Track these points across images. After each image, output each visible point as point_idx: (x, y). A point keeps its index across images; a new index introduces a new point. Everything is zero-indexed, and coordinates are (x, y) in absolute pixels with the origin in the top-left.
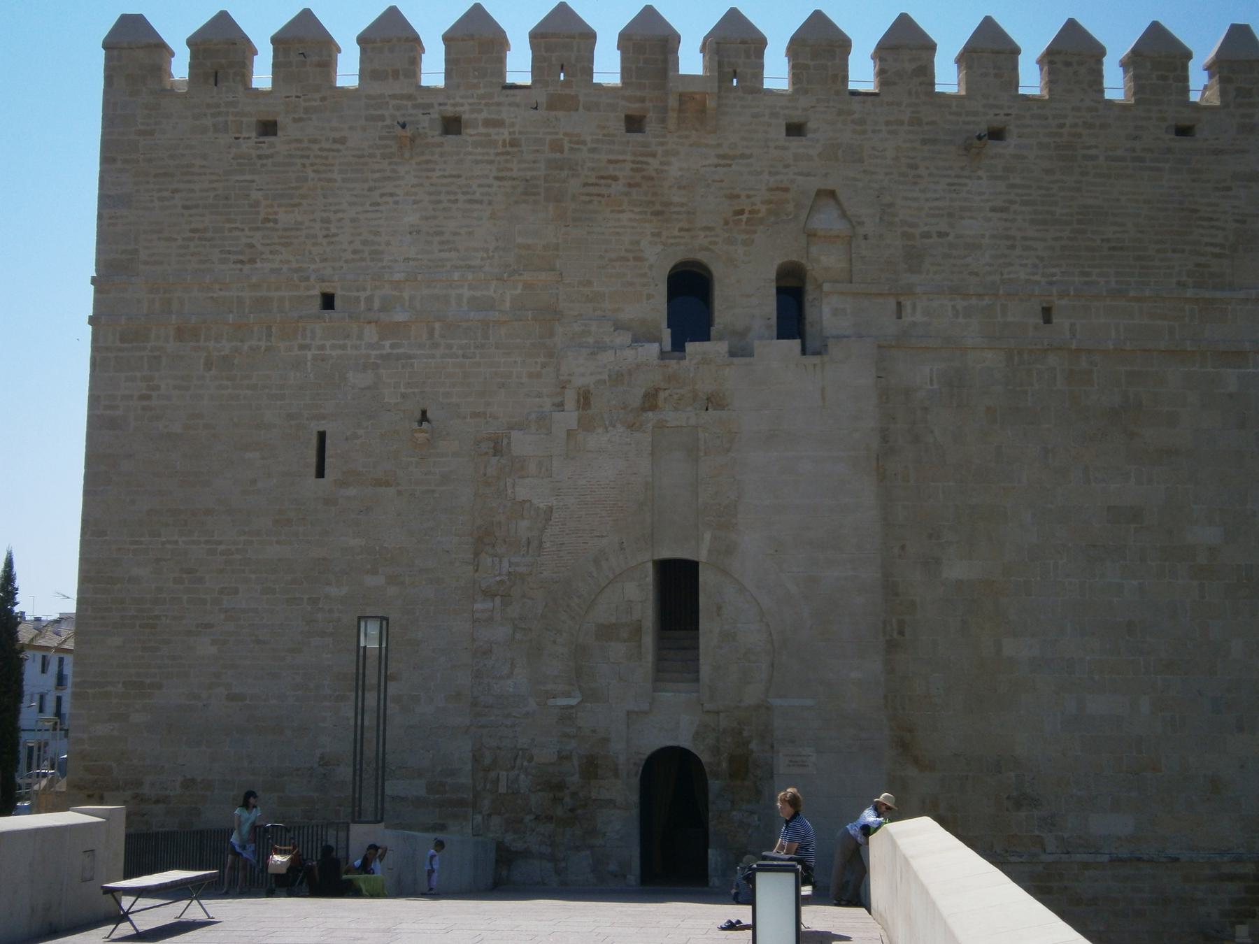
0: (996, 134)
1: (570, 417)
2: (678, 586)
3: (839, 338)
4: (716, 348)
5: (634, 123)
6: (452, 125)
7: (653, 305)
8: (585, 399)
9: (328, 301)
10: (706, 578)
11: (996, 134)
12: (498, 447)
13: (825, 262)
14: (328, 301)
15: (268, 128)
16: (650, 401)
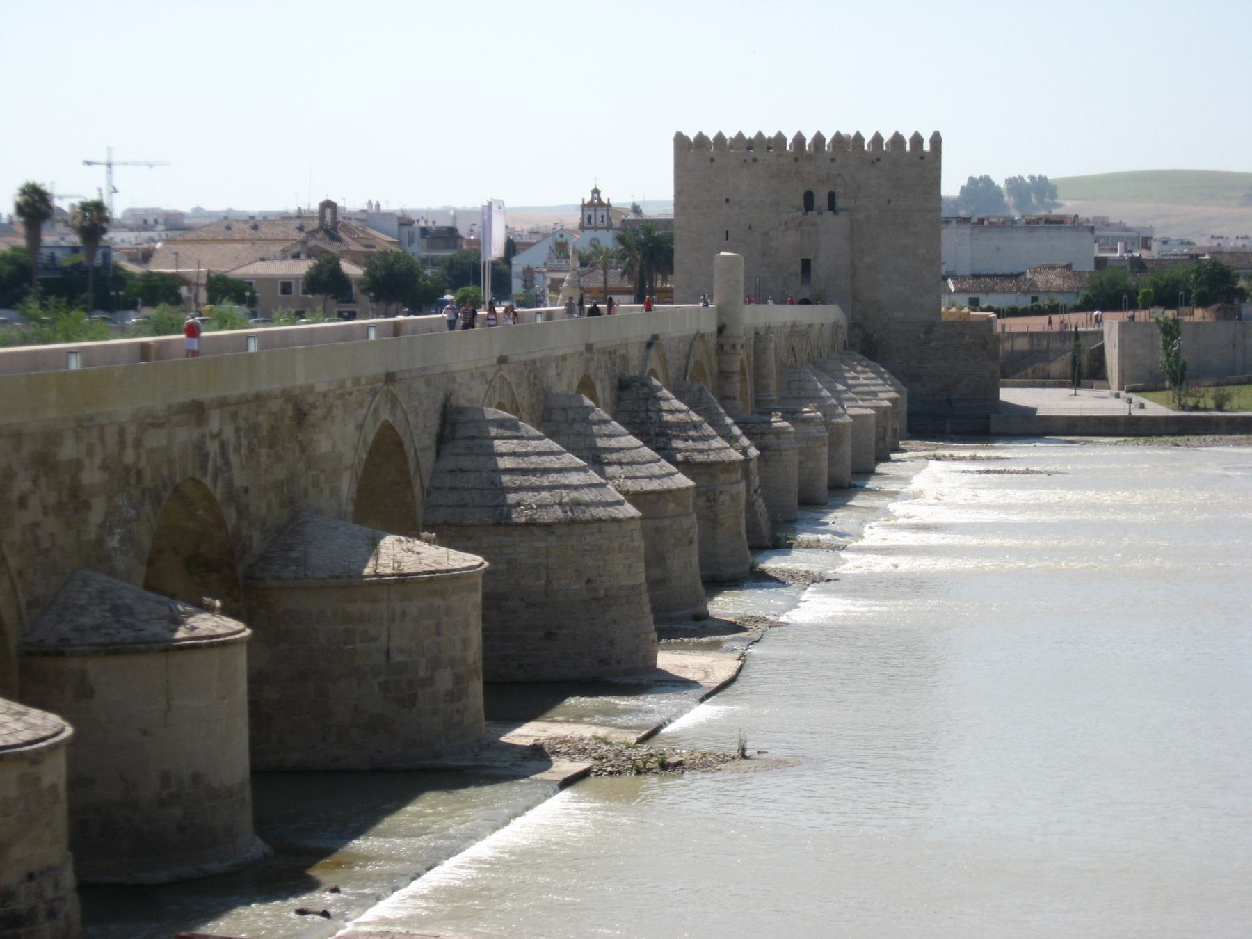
0: (878, 160)
1: (783, 227)
2: (806, 265)
3: (842, 210)
4: (815, 213)
5: (796, 160)
6: (755, 160)
7: (800, 202)
8: (786, 224)
9: (727, 200)
10: (813, 263)
11: (878, 160)
12: (767, 234)
13: (839, 190)
14: (727, 200)
15: (712, 160)
16: (800, 224)
